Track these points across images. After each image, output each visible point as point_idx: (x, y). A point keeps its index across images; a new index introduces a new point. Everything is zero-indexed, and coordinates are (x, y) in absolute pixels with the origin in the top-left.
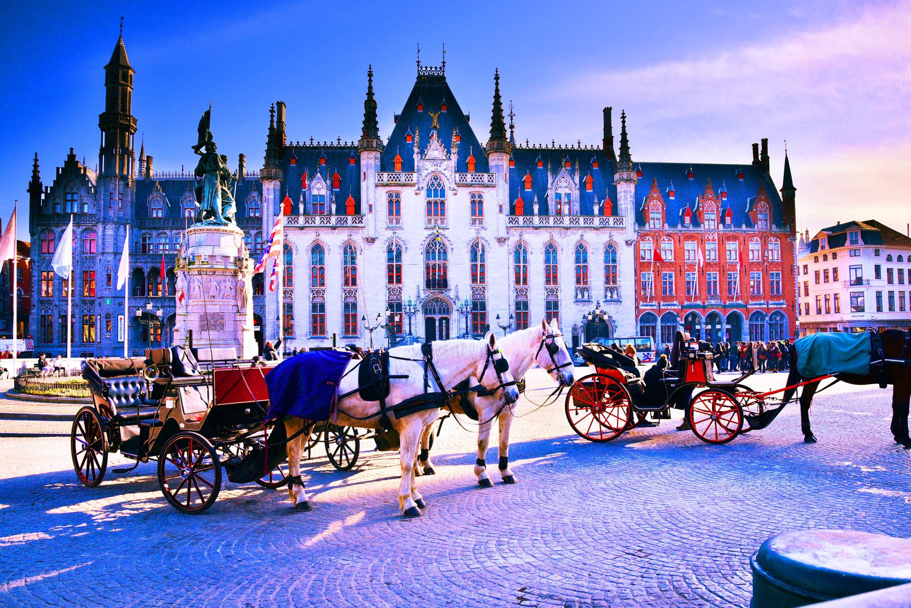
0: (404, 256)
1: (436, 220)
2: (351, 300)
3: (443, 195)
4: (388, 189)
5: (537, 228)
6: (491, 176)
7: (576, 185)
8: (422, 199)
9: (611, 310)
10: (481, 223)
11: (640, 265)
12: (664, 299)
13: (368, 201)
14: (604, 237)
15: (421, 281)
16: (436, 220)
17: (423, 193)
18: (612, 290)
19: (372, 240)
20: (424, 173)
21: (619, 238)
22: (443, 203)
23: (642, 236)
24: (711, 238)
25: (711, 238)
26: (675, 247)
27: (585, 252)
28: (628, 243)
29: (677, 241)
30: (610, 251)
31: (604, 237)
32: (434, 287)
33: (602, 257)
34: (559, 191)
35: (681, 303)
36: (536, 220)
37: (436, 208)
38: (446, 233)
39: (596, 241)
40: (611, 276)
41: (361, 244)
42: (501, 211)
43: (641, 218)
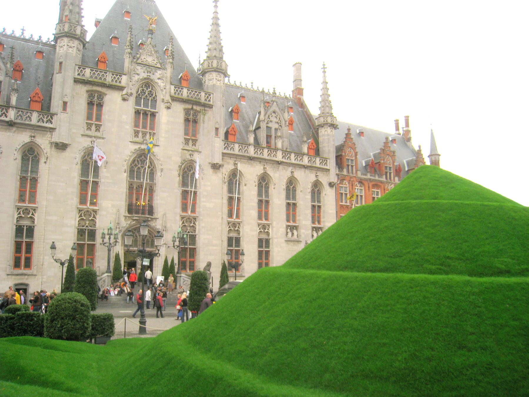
1: (144, 134)
2: (26, 223)
3: (154, 106)
4: (90, 87)
6: (208, 94)
7: (285, 122)
8: (130, 106)
10: (194, 145)
13: (63, 95)
14: (311, 177)
15: (122, 204)
16: (144, 134)
17: (132, 100)
19: (61, 147)
21: (324, 180)
22: (153, 115)
23: (342, 179)
26: (365, 193)
28: (331, 185)
29: (367, 188)
32: (137, 212)
33: (309, 197)
34: (270, 125)
36: (251, 151)
38: (155, 150)
39: (305, 180)
41: (49, 150)
42: (217, 134)
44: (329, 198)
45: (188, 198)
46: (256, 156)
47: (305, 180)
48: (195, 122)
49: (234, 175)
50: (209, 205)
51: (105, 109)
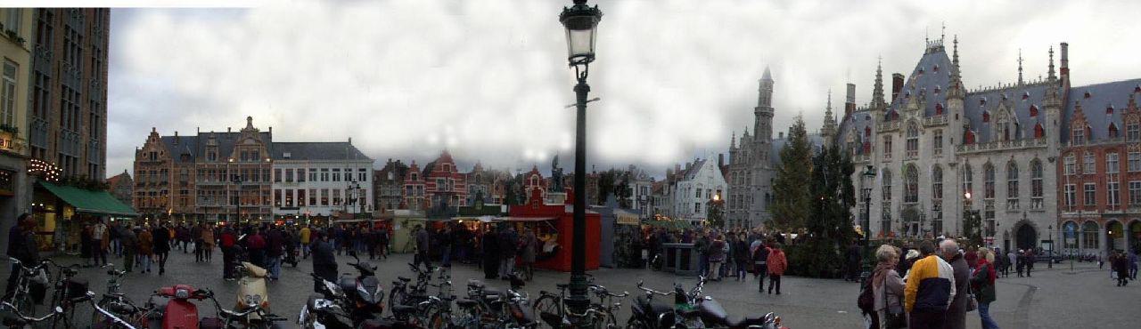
0: (893, 181)
5: (978, 154)
9: (1034, 219)
10: (941, 152)
11: (1061, 181)
12: (1087, 208)
14: (1030, 156)
17: (904, 135)
18: (1038, 200)
20: (905, 121)
21: (1043, 158)
22: (917, 140)
24: (1133, 148)
25: (1133, 148)
27: (1016, 170)
28: (1051, 160)
30: (1037, 166)
31: (1030, 156)
35: (1101, 211)
37: (912, 145)
38: (917, 162)
39: (1023, 160)
40: (1037, 189)
43: (1064, 136)
44: (1050, 172)
45: (938, 190)
46: (980, 151)
47: (1023, 160)
48: (941, 137)
49: (968, 167)
50: (949, 192)
51: (893, 144)
